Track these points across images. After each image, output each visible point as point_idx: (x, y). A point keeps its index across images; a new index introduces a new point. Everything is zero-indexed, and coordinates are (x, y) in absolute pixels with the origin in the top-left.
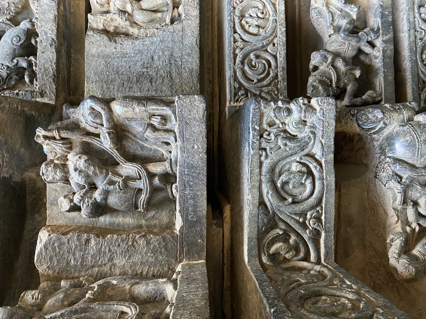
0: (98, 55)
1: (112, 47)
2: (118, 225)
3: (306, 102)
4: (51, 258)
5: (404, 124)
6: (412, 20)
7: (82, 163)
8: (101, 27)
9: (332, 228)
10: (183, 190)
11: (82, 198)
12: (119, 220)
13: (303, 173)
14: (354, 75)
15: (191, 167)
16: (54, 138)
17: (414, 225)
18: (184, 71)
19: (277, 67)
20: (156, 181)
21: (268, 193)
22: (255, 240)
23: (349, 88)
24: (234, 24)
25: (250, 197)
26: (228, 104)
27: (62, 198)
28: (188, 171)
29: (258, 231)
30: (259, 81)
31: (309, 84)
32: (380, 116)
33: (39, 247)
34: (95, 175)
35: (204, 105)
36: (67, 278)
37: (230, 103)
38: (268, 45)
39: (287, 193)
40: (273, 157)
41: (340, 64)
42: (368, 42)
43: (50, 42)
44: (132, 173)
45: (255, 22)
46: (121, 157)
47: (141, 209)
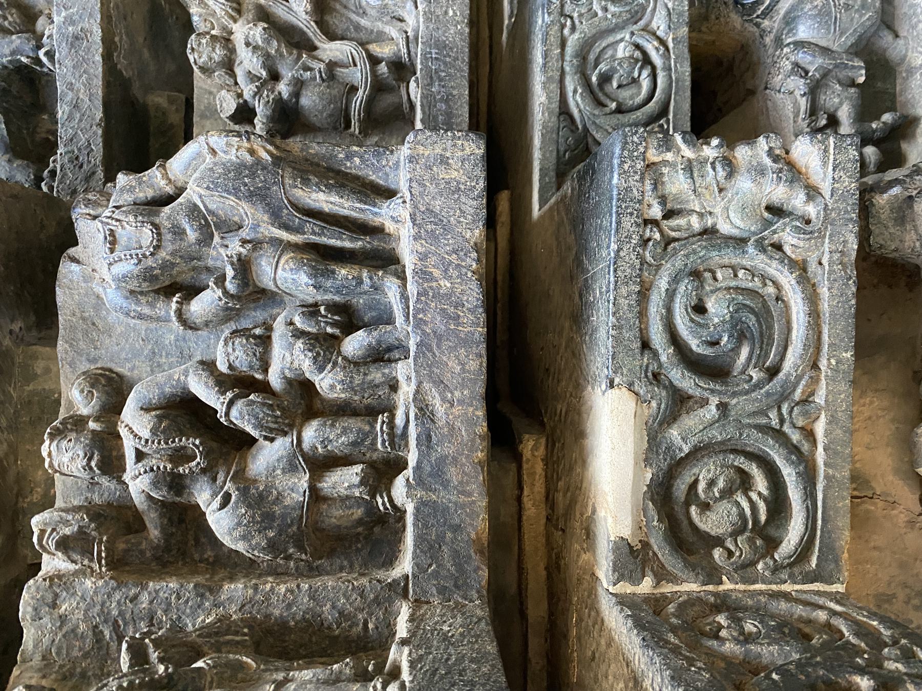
7: (258, 31)
10: (428, 85)
11: (258, 93)
13: (637, 61)
15: (441, 46)
20: (383, 68)
21: (575, 91)
22: (553, 174)
25: (543, 99)
26: (506, 22)
27: (224, 92)
28: (436, 53)
29: (558, 158)
34: (280, 56)
39: (607, 96)
40: (585, 28)
44: (341, 57)
46: (324, 34)
47: (355, 128)
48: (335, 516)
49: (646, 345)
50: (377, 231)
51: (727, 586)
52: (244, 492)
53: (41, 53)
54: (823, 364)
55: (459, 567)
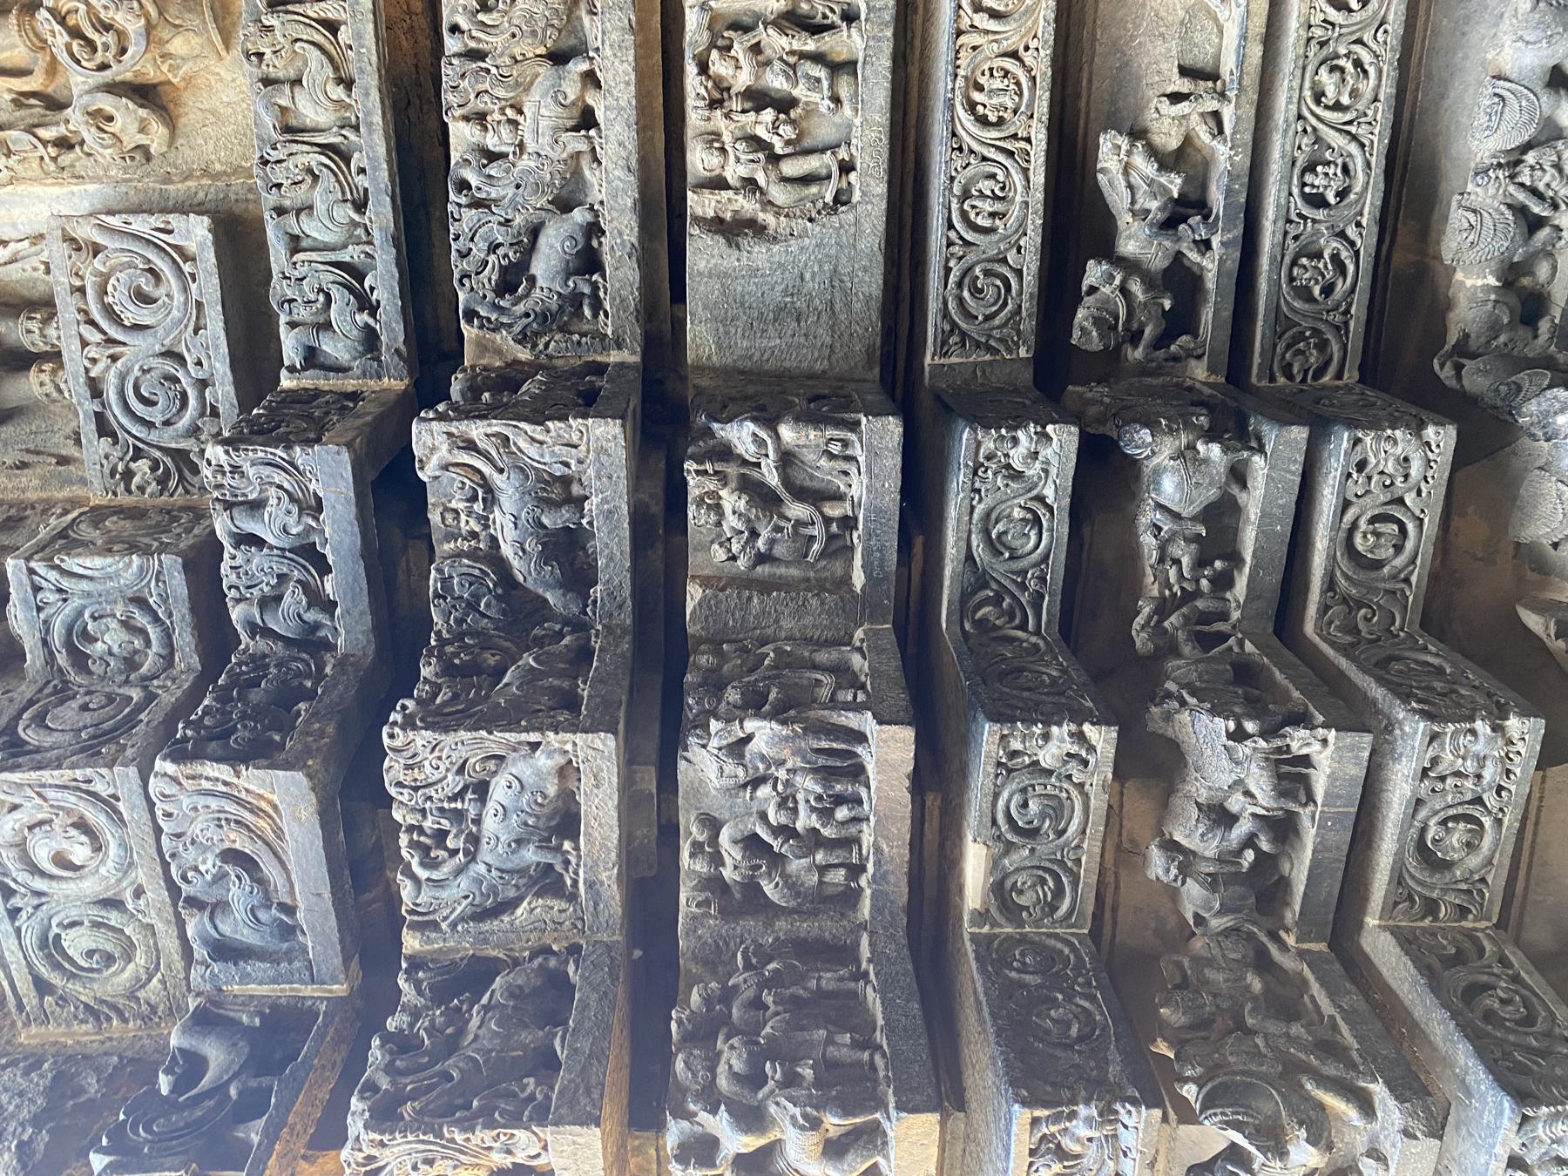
0: (710, 272)
1: (733, 259)
2: (780, 577)
3: (1039, 429)
4: (707, 618)
5: (1179, 455)
6: (1283, 201)
8: (712, 214)
9: (1059, 592)
11: (743, 549)
12: (782, 570)
14: (1162, 305)
15: (879, 511)
16: (706, 472)
17: (1176, 588)
18: (855, 299)
19: (1020, 293)
20: (834, 528)
23: (1148, 331)
24: (950, 212)
25: (954, 551)
26: (928, 360)
29: (962, 592)
30: (988, 318)
31: (1076, 321)
32: (1149, 439)
33: (690, 606)
35: (901, 430)
36: (729, 642)
37: (933, 359)
38: (1007, 250)
39: (1004, 545)
40: (989, 501)
41: (1136, 287)
42: (1195, 241)
43: (628, 250)
45: (987, 206)
48: (830, 891)
49: (994, 822)
50: (855, 755)
51: (1027, 929)
52: (786, 882)
53: (584, 522)
54: (1088, 831)
55: (893, 918)
